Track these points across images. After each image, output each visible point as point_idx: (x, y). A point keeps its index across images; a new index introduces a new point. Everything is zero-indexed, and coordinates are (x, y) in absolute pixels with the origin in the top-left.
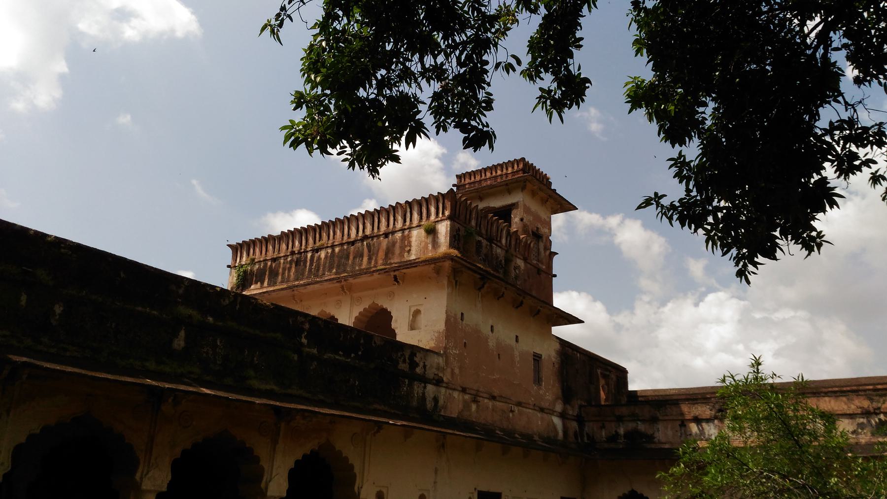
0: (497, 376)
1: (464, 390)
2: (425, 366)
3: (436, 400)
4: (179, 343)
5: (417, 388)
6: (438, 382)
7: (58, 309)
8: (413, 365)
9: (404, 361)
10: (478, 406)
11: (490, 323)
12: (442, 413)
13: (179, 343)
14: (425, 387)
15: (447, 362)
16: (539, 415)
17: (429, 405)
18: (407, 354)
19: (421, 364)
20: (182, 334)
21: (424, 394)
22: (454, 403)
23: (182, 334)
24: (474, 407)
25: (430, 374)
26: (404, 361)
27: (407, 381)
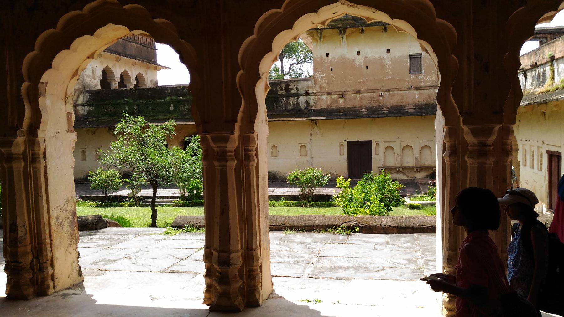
0: (364, 79)
1: (329, 94)
2: (297, 89)
3: (307, 103)
4: (172, 108)
5: (292, 100)
6: (307, 94)
7: (136, 107)
8: (288, 90)
9: (282, 90)
10: (345, 99)
11: (357, 50)
12: (313, 108)
13: (172, 108)
14: (298, 99)
15: (315, 82)
16: (416, 92)
17: (302, 106)
18: (283, 86)
19: (295, 88)
20: (172, 105)
21: (297, 102)
22: (325, 102)
23: (172, 105)
24: (341, 101)
25: (302, 91)
26: (282, 90)
27: (284, 99)
